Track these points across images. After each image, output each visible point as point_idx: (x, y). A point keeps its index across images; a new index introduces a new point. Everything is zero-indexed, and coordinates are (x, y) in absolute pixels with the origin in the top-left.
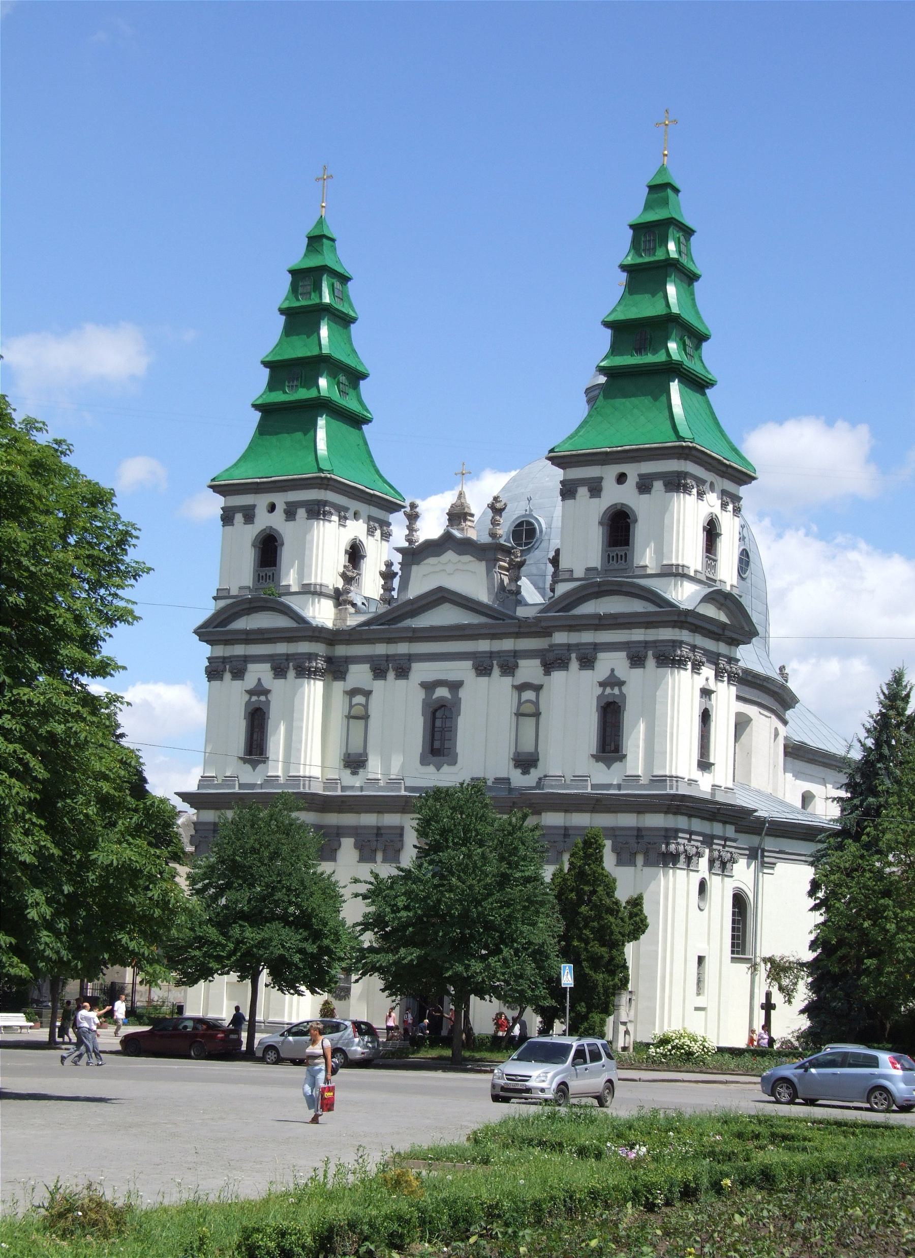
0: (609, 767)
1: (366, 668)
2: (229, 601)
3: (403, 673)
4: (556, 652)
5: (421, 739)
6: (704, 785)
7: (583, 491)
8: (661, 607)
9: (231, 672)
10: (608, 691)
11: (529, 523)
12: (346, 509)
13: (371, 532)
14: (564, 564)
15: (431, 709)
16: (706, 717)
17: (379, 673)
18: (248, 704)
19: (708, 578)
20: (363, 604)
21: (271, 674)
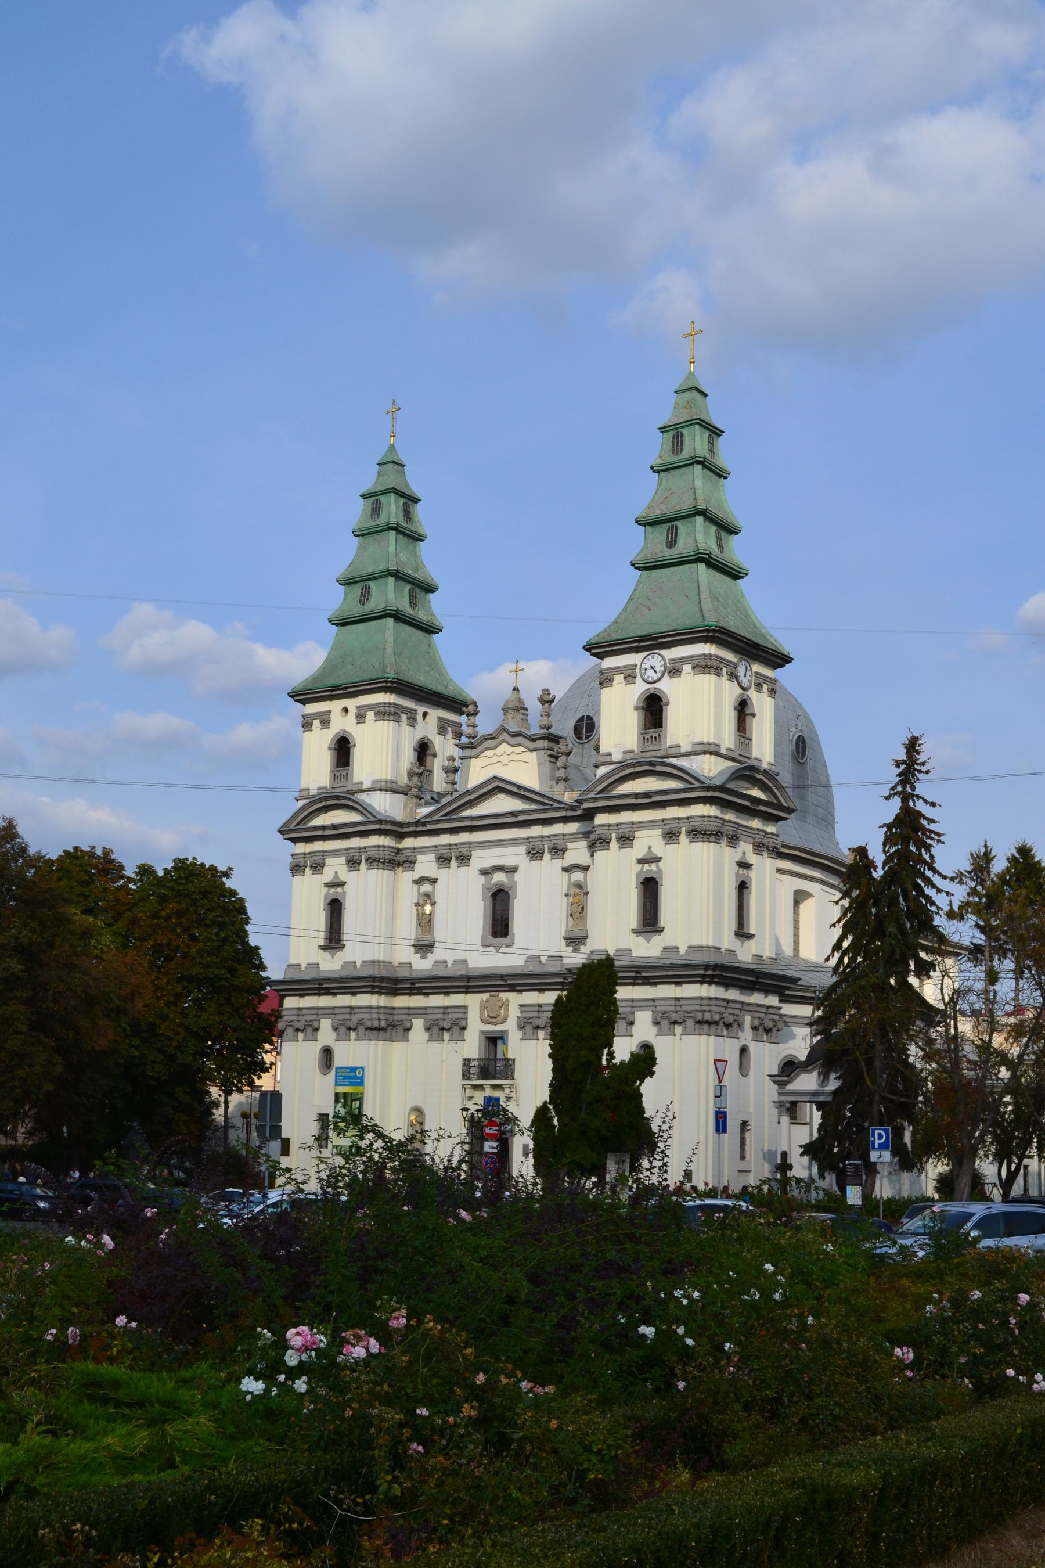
0: (648, 941)
1: (432, 857)
2: (308, 801)
3: (464, 859)
4: (597, 832)
5: (481, 922)
6: (745, 954)
7: (619, 679)
8: (690, 783)
9: (311, 867)
10: (646, 867)
11: (589, 718)
12: (415, 711)
13: (442, 731)
14: (603, 749)
15: (491, 893)
16: (742, 887)
17: (443, 861)
18: (326, 895)
19: (740, 755)
20: (432, 798)
21: (345, 868)
